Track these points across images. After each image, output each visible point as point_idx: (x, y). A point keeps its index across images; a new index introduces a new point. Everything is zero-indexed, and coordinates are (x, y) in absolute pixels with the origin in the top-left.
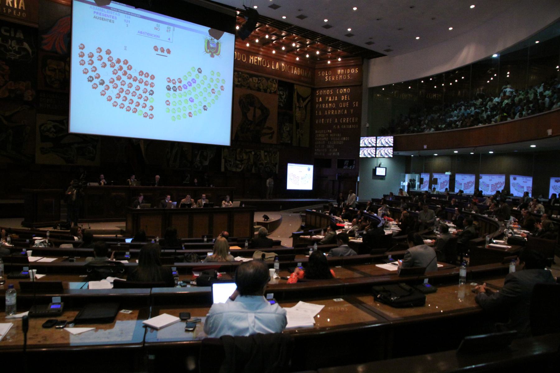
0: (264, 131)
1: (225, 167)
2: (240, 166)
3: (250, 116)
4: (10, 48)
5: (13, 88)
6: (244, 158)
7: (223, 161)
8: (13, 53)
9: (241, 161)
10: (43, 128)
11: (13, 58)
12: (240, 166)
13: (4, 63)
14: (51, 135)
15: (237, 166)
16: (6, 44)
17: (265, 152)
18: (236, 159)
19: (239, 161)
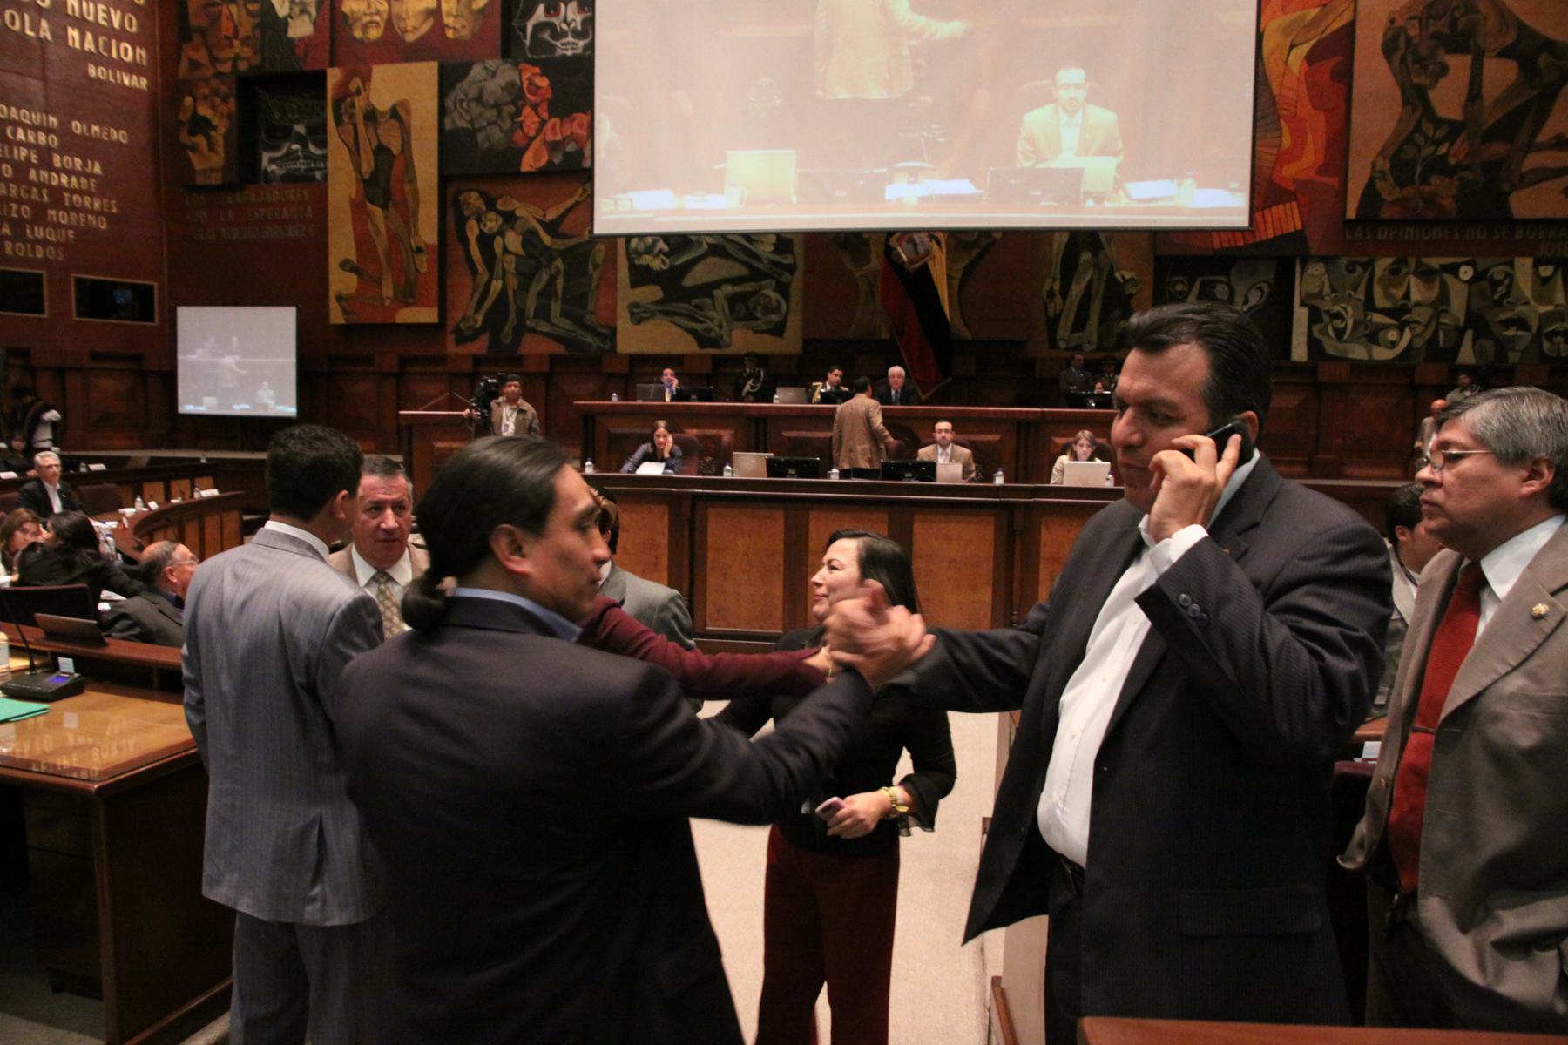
0: (1534, 161)
1: (1314, 345)
2: (1392, 335)
3: (1448, 99)
4: (564, 26)
5: (559, 138)
6: (1415, 296)
7: (1301, 315)
8: (570, 39)
9: (1399, 313)
10: (634, 243)
11: (569, 53)
12: (1392, 335)
13: (537, 70)
14: (656, 264)
15: (1373, 338)
16: (554, 20)
17: (1536, 264)
18: (1369, 305)
19: (1383, 312)
